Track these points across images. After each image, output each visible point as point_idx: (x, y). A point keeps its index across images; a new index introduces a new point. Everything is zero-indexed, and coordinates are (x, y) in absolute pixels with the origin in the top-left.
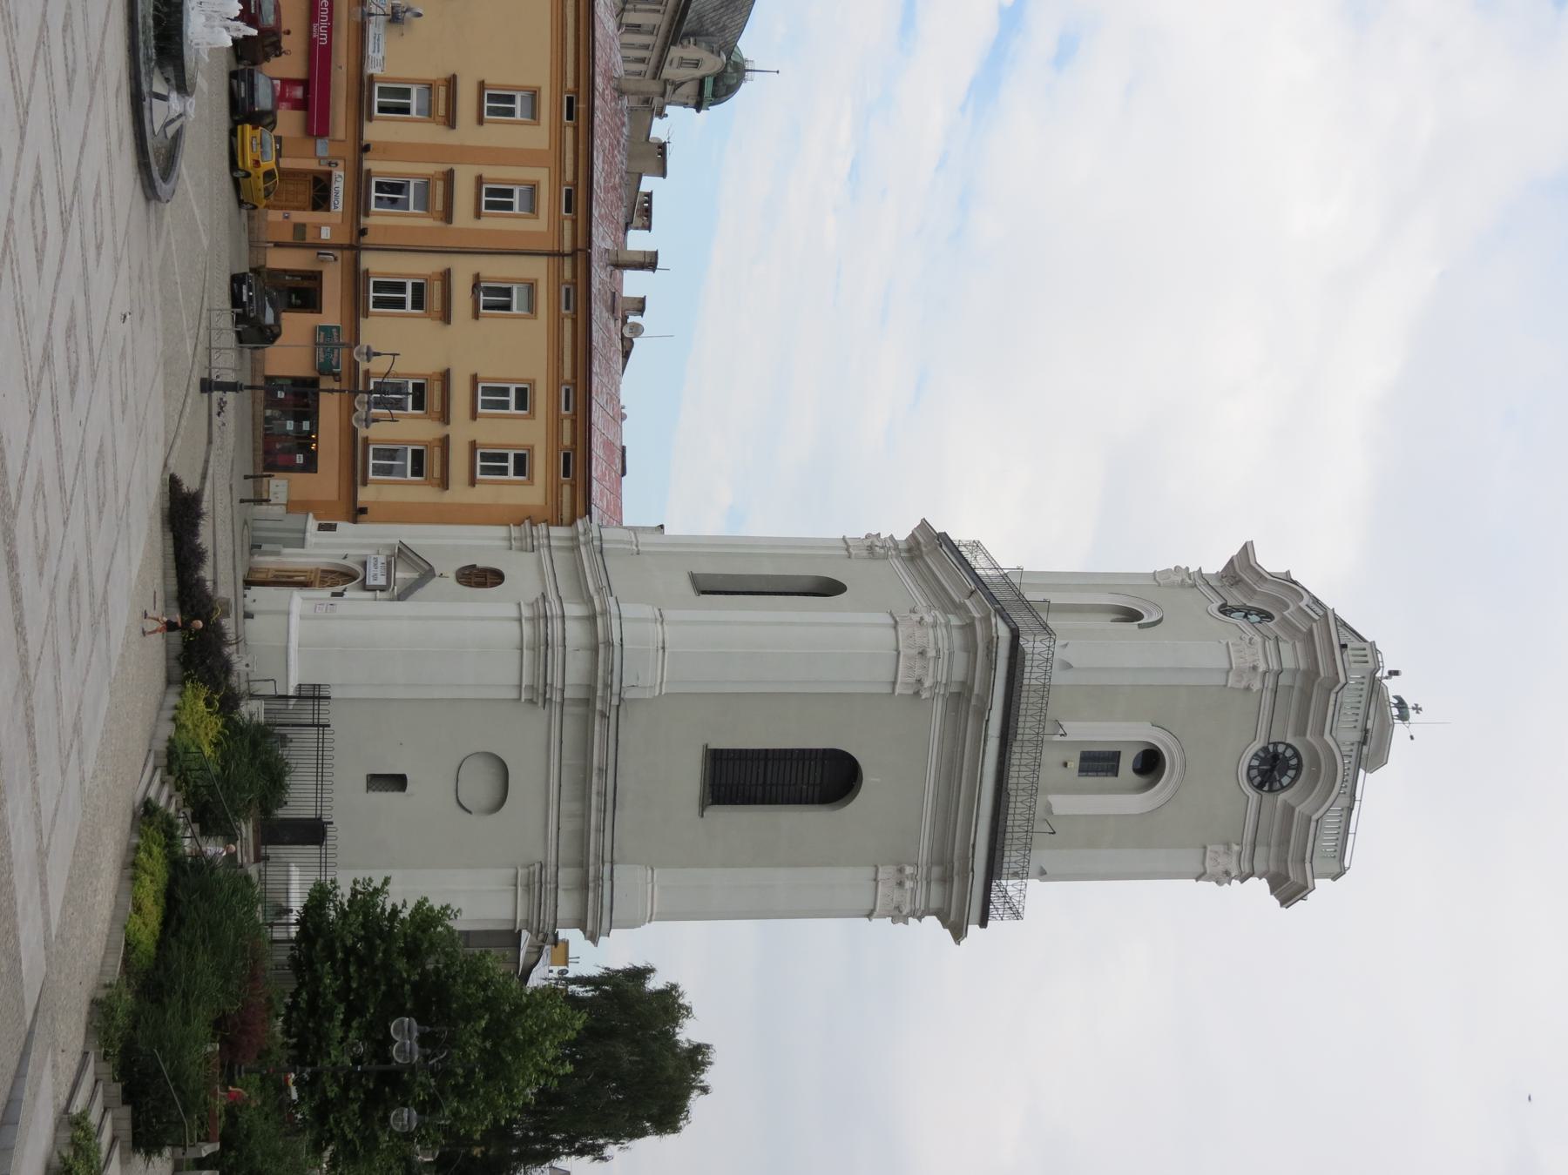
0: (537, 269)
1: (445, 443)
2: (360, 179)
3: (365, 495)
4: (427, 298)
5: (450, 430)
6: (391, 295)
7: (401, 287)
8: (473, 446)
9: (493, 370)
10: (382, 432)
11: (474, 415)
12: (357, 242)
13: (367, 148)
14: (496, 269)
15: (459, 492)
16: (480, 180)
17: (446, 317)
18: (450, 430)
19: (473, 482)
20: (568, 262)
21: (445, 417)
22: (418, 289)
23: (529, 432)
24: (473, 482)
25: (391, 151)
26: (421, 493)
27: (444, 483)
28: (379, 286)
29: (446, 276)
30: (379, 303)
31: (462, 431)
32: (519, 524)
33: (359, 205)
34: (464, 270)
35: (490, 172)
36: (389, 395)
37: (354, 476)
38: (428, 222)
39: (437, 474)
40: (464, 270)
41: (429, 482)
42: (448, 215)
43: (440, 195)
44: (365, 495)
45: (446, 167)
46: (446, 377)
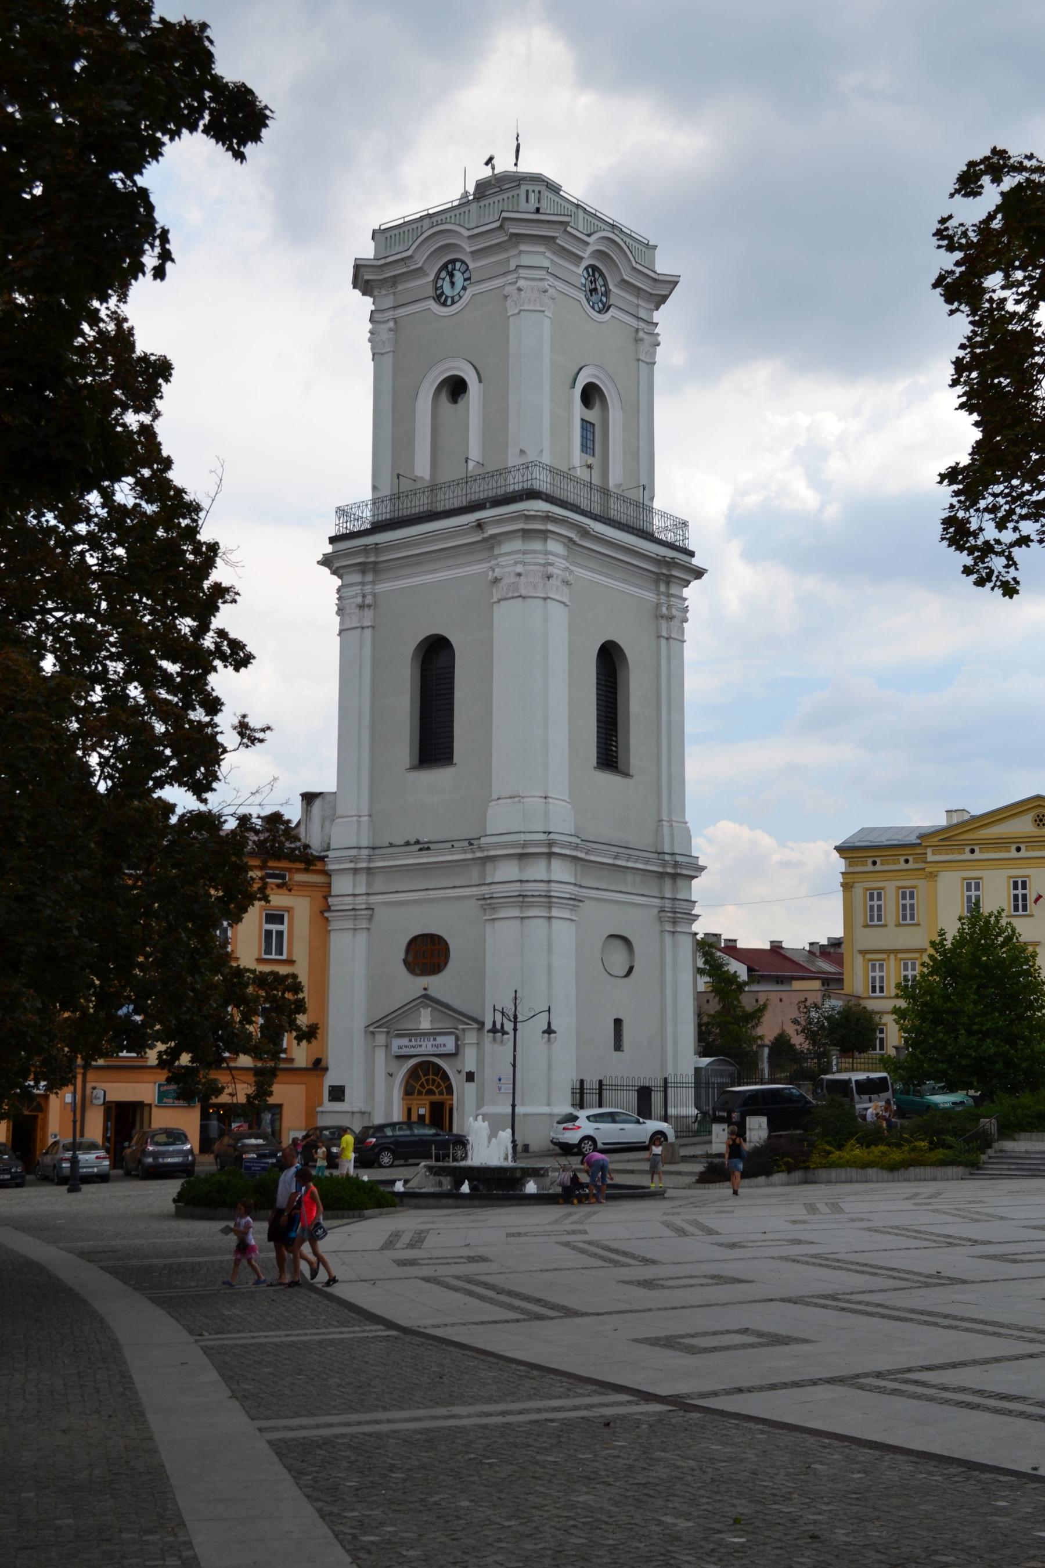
24: (290, 962)
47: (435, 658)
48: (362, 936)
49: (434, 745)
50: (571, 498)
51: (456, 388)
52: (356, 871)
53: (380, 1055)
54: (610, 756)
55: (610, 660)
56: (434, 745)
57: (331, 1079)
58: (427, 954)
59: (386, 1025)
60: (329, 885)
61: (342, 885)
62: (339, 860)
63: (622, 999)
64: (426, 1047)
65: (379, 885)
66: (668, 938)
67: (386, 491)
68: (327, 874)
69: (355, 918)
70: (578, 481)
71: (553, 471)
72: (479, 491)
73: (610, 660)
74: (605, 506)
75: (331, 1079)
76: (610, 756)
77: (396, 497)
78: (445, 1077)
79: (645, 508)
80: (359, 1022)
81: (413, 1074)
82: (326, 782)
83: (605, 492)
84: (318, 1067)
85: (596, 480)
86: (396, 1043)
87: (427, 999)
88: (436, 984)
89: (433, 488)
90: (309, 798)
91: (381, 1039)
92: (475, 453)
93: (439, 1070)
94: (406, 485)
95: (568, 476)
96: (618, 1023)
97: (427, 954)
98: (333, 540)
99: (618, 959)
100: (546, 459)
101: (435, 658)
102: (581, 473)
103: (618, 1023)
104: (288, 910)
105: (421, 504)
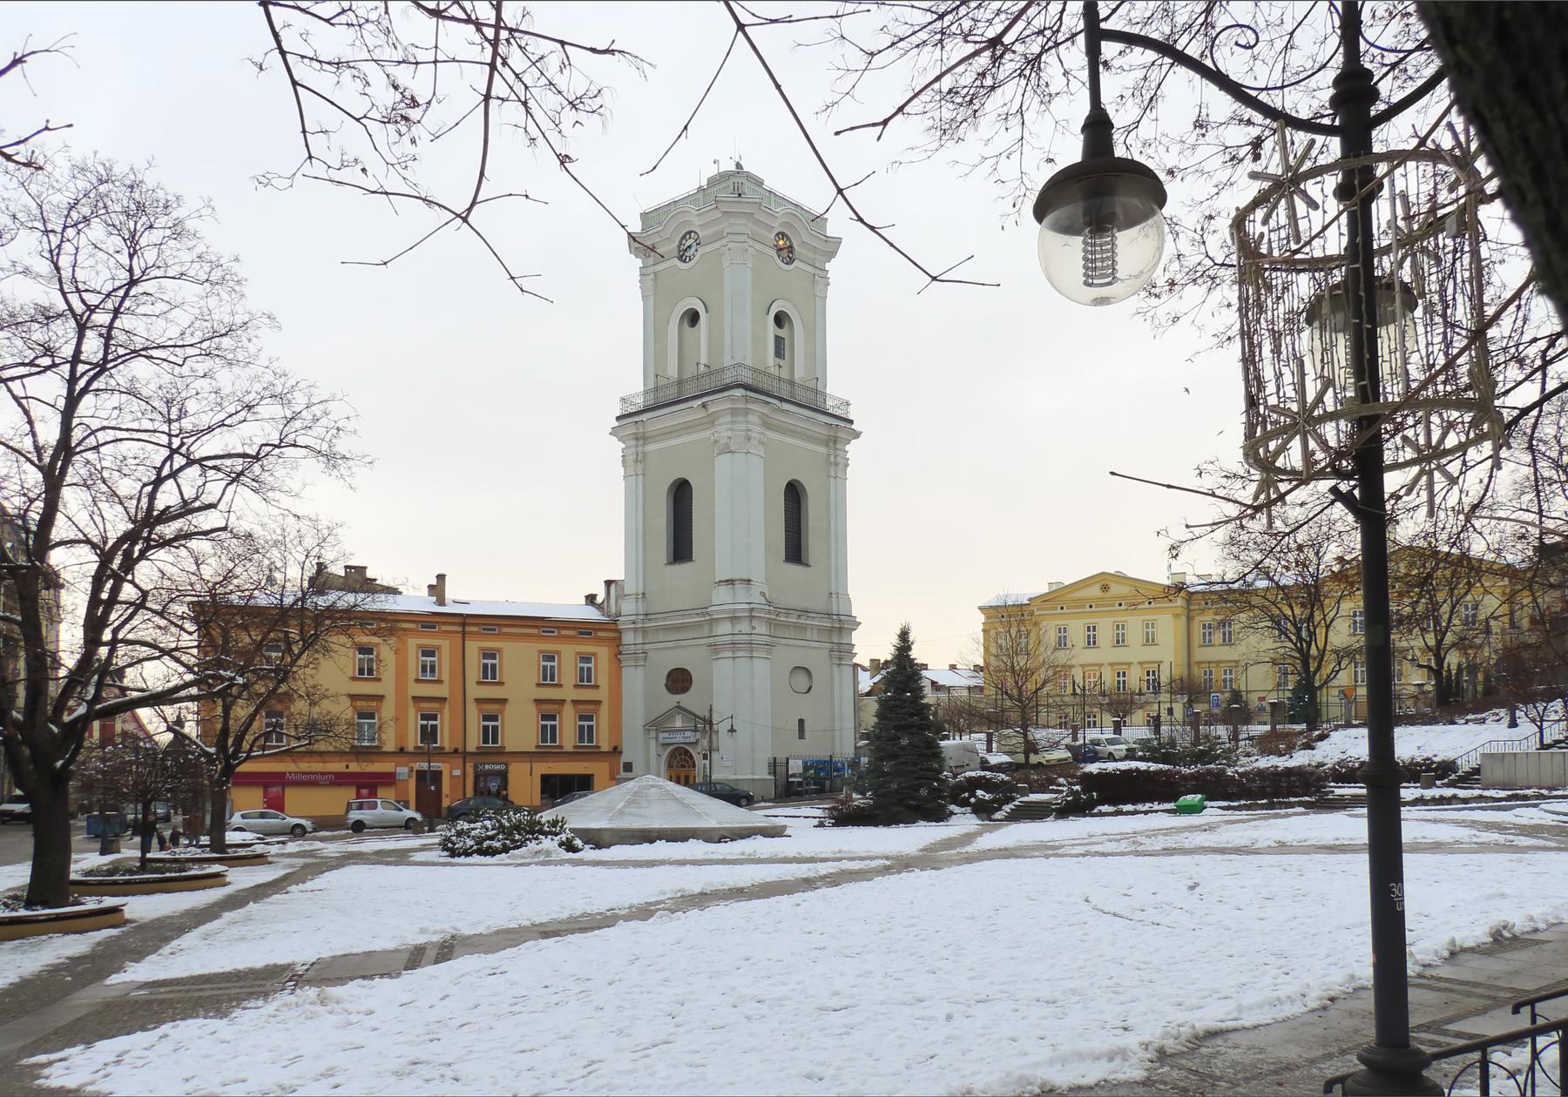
0: (473, 647)
1: (575, 702)
2: (418, 754)
3: (605, 747)
4: (492, 711)
5: (569, 699)
6: (490, 734)
7: (486, 728)
8: (576, 686)
9: (535, 677)
10: (568, 738)
11: (559, 685)
12: (460, 754)
13: (402, 750)
14: (474, 673)
15: (602, 694)
16: (417, 681)
17: (504, 701)
18: (569, 699)
19: (597, 687)
20: (468, 629)
21: (562, 702)
22: (486, 718)
23: (568, 653)
24: (597, 687)
25: (401, 735)
26: (604, 711)
27: (599, 702)
28: (486, 741)
29: (479, 701)
30: (495, 741)
31: (569, 693)
32: (620, 661)
33: (441, 753)
34: (475, 691)
35: (412, 675)
36: (548, 733)
37: (594, 754)
38: (446, 711)
39: (592, 707)
40: (475, 691)
41: (597, 711)
42: (443, 700)
43: (429, 709)
44: (605, 747)
45: (411, 703)
46: (538, 702)
47: (681, 493)
48: (640, 669)
49: (681, 549)
50: (766, 387)
51: (693, 318)
52: (635, 630)
53: (653, 743)
54: (795, 551)
55: (794, 494)
56: (681, 549)
57: (625, 758)
58: (679, 680)
59: (656, 725)
60: (620, 638)
61: (628, 638)
62: (625, 622)
63: (804, 707)
64: (679, 738)
65: (650, 638)
66: (836, 669)
67: (651, 386)
68: (619, 631)
69: (636, 660)
70: (770, 375)
71: (754, 370)
72: (707, 384)
73: (794, 494)
74: (792, 394)
75: (625, 758)
76: (795, 551)
77: (656, 389)
78: (691, 757)
79: (820, 393)
80: (640, 723)
81: (672, 755)
82: (618, 575)
83: (792, 383)
84: (616, 751)
85: (784, 374)
86: (662, 735)
87: (680, 708)
88: (685, 699)
89: (680, 382)
90: (608, 583)
91: (653, 734)
92: (704, 360)
93: (687, 752)
94: (662, 382)
95: (764, 373)
96: (801, 722)
97: (679, 680)
98: (618, 418)
99: (801, 681)
100: (749, 362)
101: (681, 493)
102: (774, 371)
103: (801, 722)
104: (595, 654)
105: (672, 393)
